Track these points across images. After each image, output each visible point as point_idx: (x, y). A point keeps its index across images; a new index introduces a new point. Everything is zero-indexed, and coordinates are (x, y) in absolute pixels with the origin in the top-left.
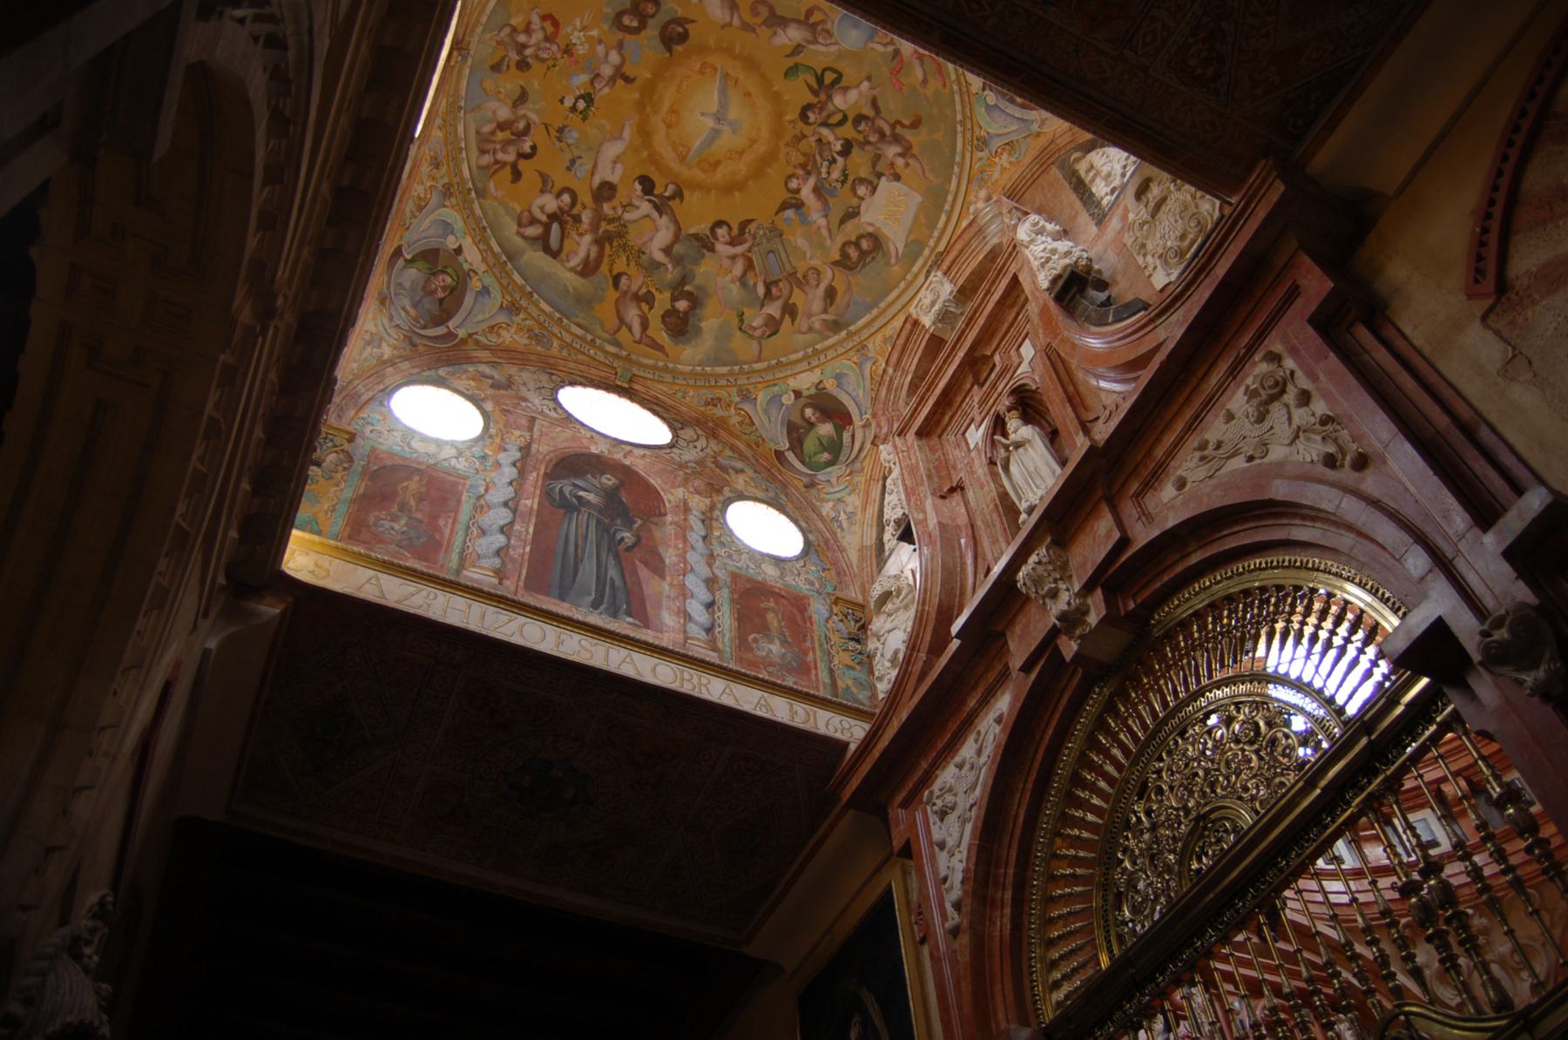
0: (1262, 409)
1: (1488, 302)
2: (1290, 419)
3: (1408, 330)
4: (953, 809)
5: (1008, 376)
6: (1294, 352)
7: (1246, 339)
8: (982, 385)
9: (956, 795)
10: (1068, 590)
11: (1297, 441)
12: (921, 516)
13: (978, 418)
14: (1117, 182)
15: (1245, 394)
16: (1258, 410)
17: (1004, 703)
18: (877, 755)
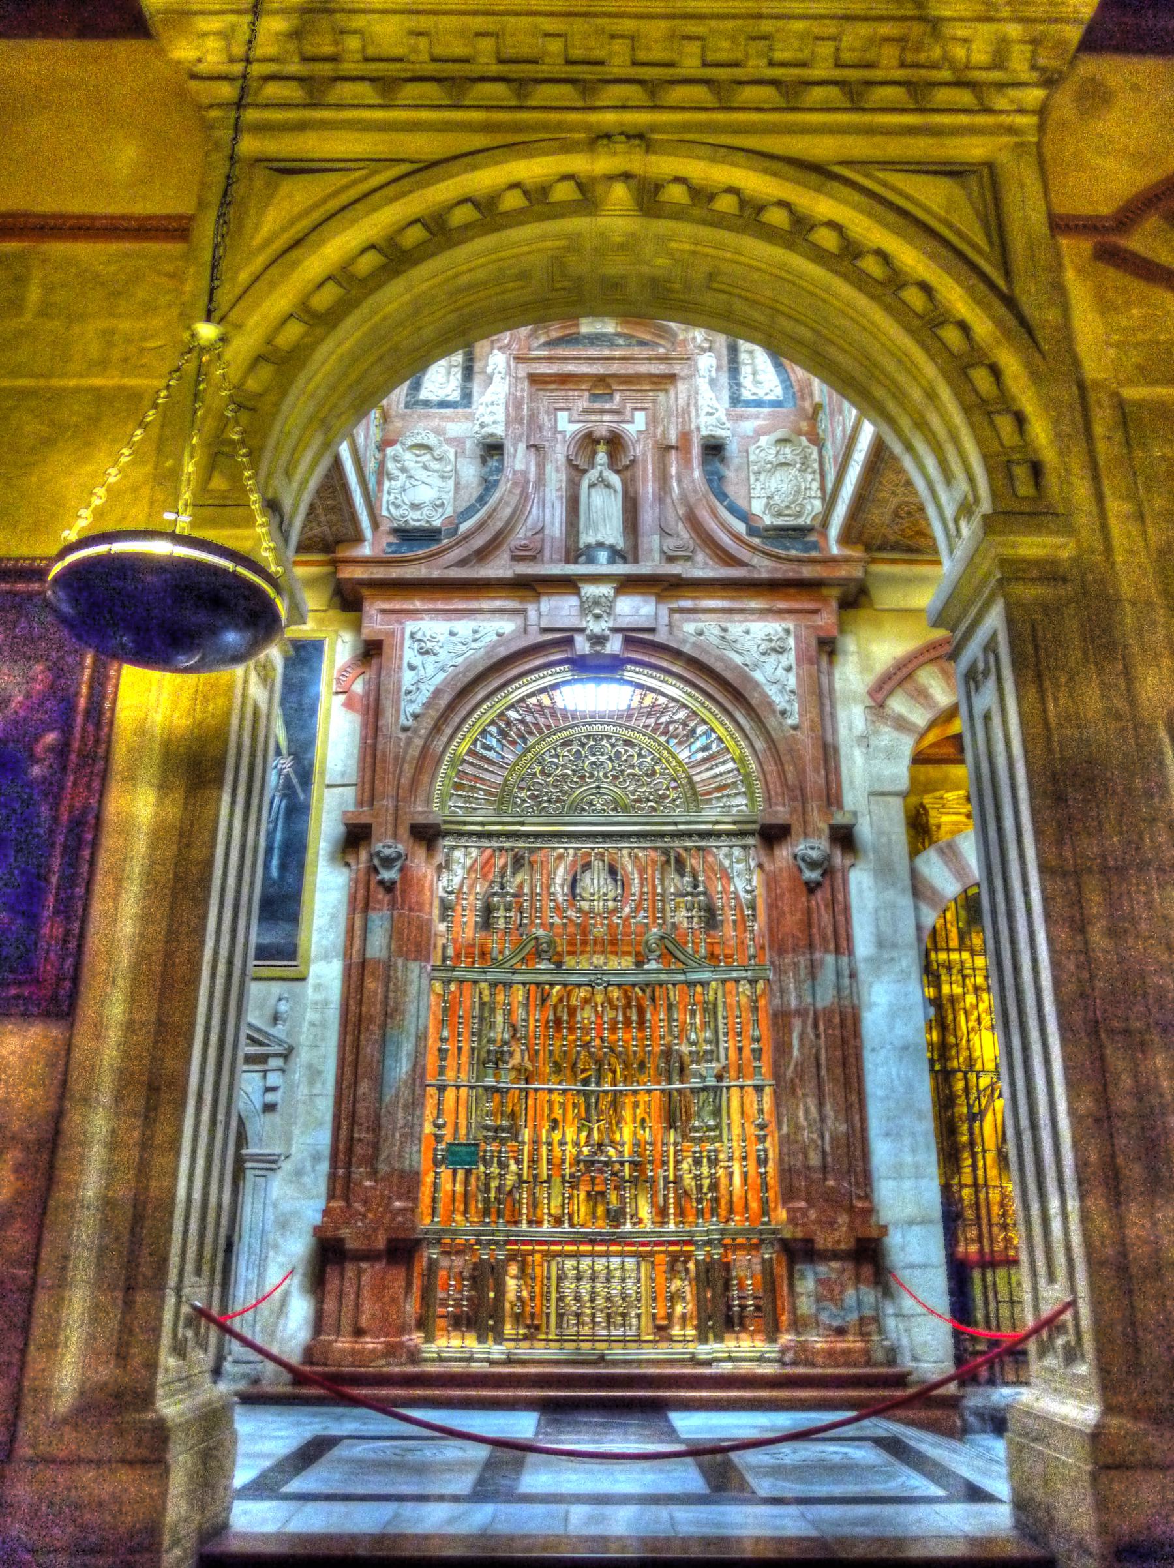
5: (616, 418)
6: (797, 639)
8: (594, 397)
12: (512, 450)
13: (576, 417)
14: (761, 393)
17: (508, 626)
18: (394, 575)
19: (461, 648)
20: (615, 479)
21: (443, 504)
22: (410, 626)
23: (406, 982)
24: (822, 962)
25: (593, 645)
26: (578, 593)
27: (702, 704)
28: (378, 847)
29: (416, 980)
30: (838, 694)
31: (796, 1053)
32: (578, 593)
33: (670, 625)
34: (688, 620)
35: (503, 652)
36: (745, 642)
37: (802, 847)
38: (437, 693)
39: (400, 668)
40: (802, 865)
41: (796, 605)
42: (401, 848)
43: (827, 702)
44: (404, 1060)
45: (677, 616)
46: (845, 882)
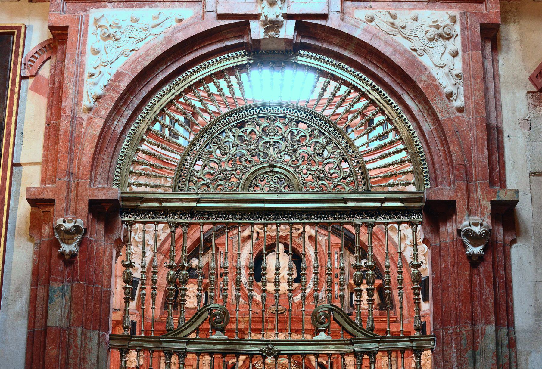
0: (436, 37)
1: (535, 89)
2: (443, 54)
3: (501, 62)
9: (122, 33)
10: (280, 8)
11: (441, 68)
15: (434, 22)
16: (434, 36)
22: (94, 13)
23: (85, 350)
24: (483, 331)
25: (267, 30)
27: (373, 88)
28: (60, 221)
29: (95, 349)
30: (502, 79)
34: (358, 8)
35: (181, 37)
36: (412, 27)
37: (466, 223)
38: (118, 76)
39: (83, 53)
40: (466, 241)
42: (80, 222)
43: (491, 86)
46: (507, 257)
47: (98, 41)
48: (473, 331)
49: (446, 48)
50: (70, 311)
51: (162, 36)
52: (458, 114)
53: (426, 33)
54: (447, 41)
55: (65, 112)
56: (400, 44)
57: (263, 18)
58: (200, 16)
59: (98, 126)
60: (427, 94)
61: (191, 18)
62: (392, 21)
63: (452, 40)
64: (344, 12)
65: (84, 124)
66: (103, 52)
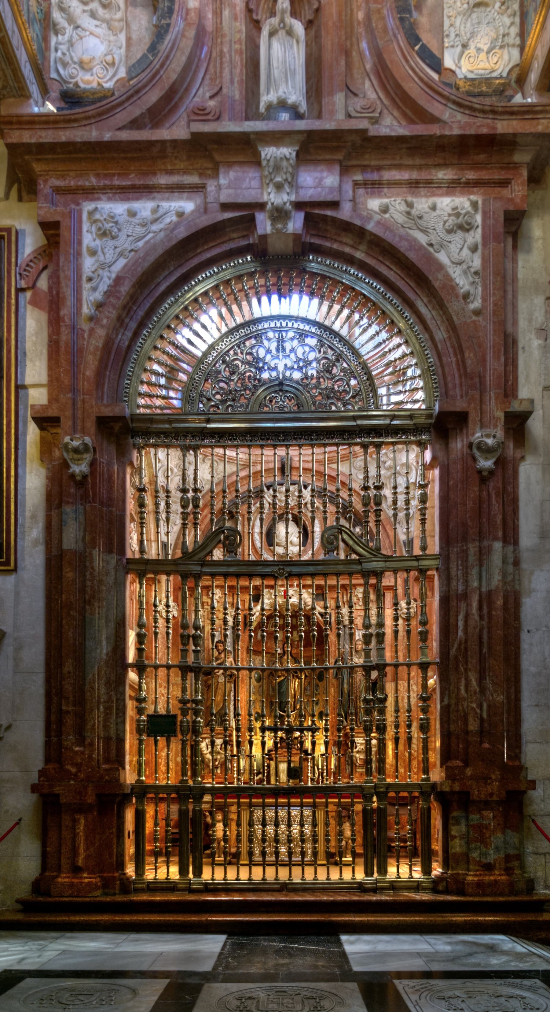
4: (113, 238)
7: (471, 175)
9: (119, 230)
19: (139, 230)
20: (299, 27)
21: (113, 64)
22: (88, 206)
26: (257, 162)
31: (460, 633)
32: (257, 162)
33: (354, 200)
34: (373, 195)
35: (182, 233)
38: (118, 280)
40: (477, 454)
41: (484, 175)
44: (104, 643)
45: (361, 191)
47: (94, 240)
48: (480, 547)
49: (465, 241)
50: (85, 534)
51: (162, 234)
52: (474, 318)
53: (445, 222)
54: (467, 234)
55: (64, 322)
56: (415, 240)
57: (269, 206)
58: (202, 210)
59: (100, 337)
60: (443, 294)
61: (193, 212)
62: (408, 209)
63: (472, 232)
64: (357, 201)
65: (86, 336)
66: (100, 253)
